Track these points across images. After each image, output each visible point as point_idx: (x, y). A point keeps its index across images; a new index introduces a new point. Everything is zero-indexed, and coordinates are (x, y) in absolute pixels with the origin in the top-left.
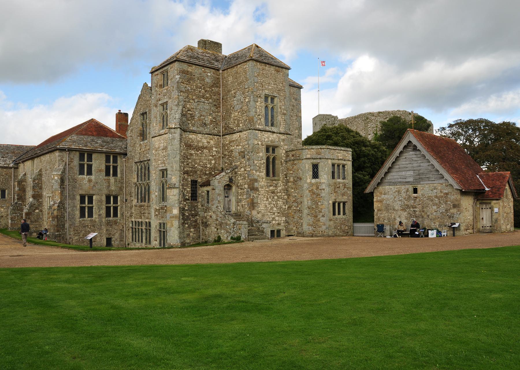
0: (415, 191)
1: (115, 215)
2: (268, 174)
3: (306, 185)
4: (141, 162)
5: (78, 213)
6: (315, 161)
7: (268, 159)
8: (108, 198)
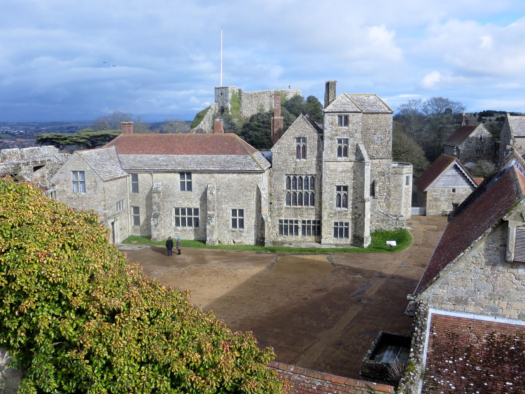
0: (454, 190)
3: (403, 190)
4: (296, 175)
6: (407, 175)
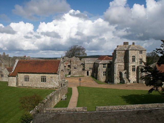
1: (110, 75)
2: (133, 71)
5: (103, 75)
7: (133, 68)
8: (109, 72)
